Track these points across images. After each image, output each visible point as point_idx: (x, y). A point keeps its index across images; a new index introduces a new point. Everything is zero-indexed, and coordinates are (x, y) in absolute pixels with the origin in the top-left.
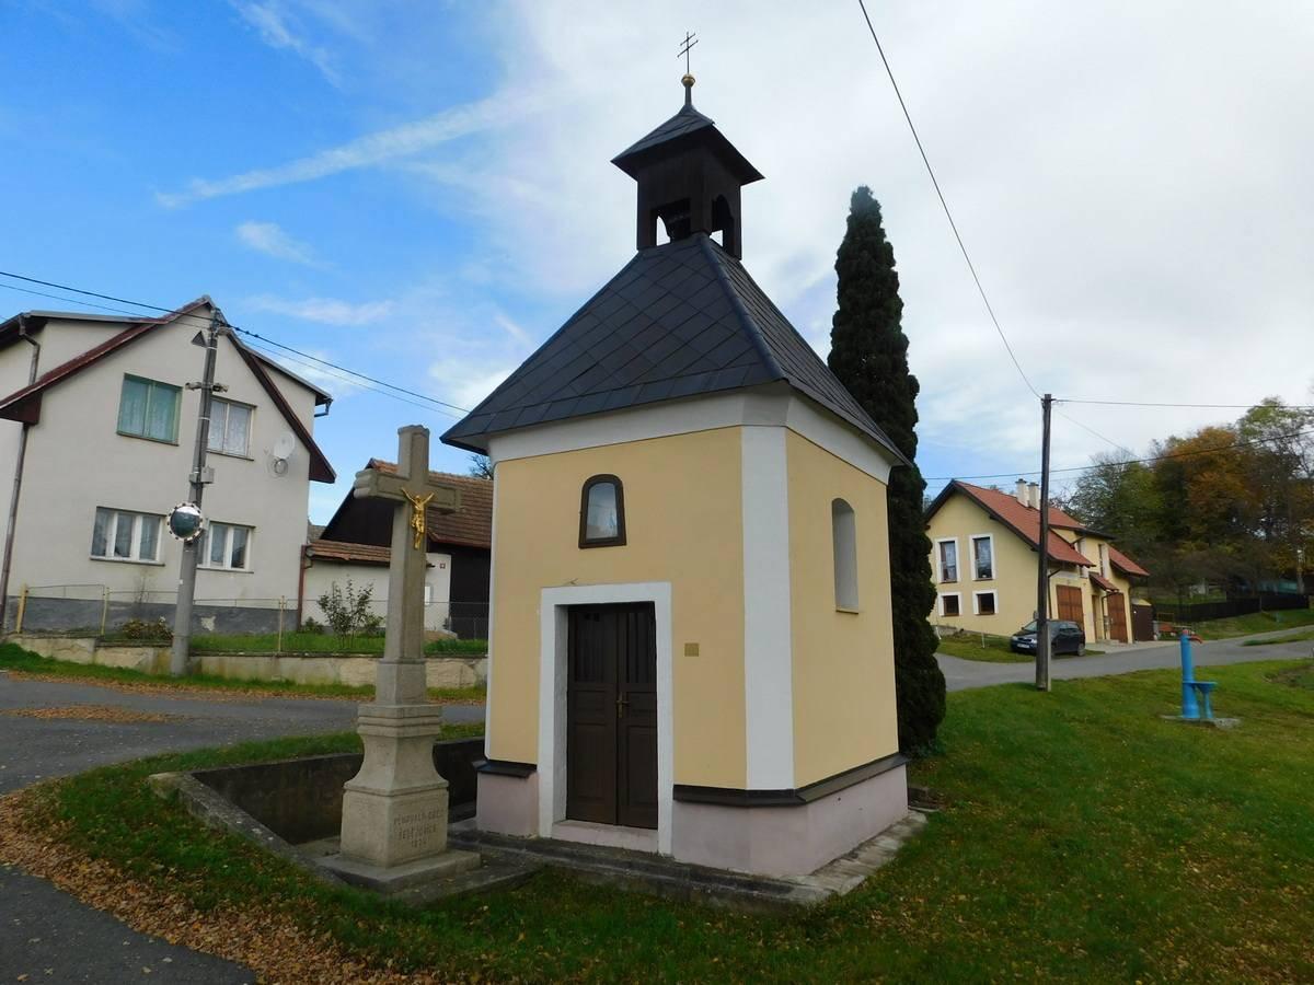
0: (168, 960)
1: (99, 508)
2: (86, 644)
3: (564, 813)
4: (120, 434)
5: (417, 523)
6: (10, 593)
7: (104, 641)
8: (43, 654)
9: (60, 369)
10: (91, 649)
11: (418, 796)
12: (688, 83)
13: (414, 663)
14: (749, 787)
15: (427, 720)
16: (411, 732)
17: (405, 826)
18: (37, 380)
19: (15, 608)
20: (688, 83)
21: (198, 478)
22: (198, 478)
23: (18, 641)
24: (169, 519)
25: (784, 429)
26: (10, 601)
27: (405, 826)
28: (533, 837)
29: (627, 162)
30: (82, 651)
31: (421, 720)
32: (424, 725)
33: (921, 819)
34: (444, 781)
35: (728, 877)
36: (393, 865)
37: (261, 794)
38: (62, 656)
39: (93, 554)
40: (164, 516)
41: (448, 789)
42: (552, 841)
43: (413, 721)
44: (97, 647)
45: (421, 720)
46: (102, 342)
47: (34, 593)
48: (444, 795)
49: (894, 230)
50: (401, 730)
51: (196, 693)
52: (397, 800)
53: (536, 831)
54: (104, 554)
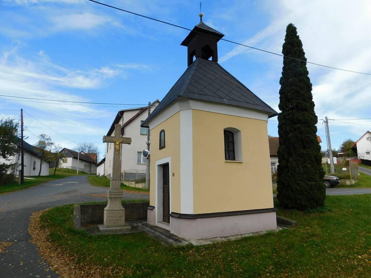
0: (22, 235)
1: (138, 152)
2: (134, 183)
3: (162, 220)
4: (141, 134)
5: (117, 147)
6: (122, 172)
7: (137, 182)
8: (127, 185)
9: (127, 122)
10: (134, 184)
11: (115, 211)
12: (201, 16)
13: (116, 180)
14: (181, 213)
15: (118, 194)
16: (113, 196)
17: (111, 218)
18: (123, 124)
19: (123, 175)
20: (201, 16)
21: (148, 143)
22: (148, 143)
23: (123, 183)
24: (142, 153)
25: (191, 110)
26: (122, 174)
27: (111, 218)
28: (154, 225)
29: (184, 44)
30: (133, 185)
31: (116, 194)
32: (117, 195)
33: (90, 208)
34: (124, 208)
35: (176, 238)
36: (107, 227)
37: (98, 211)
38: (130, 186)
39: (138, 162)
40: (142, 152)
41: (125, 210)
42: (157, 227)
43: (114, 194)
44: (135, 183)
45: (116, 194)
46: (135, 114)
47: (126, 172)
48: (123, 212)
49: (301, 34)
50: (110, 196)
51: (59, 184)
52: (108, 212)
53: (155, 224)
54: (140, 162)
